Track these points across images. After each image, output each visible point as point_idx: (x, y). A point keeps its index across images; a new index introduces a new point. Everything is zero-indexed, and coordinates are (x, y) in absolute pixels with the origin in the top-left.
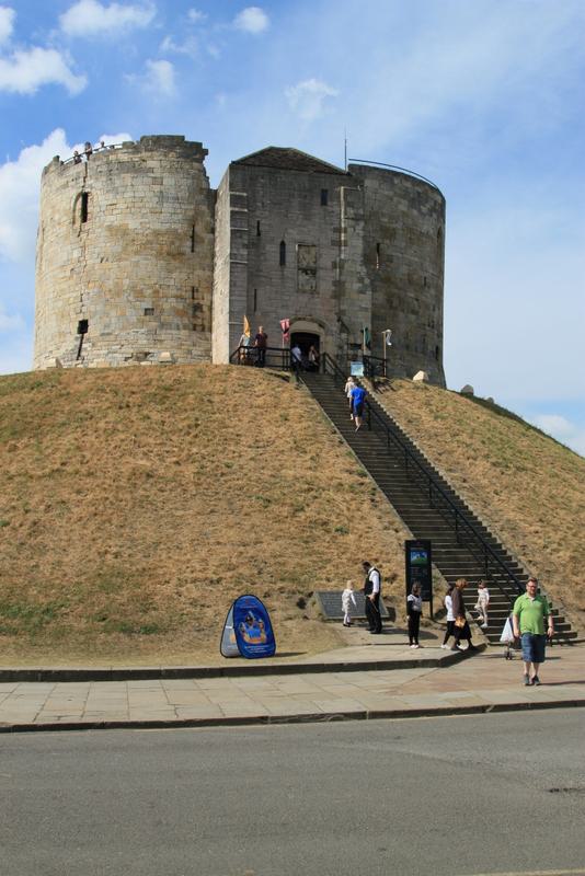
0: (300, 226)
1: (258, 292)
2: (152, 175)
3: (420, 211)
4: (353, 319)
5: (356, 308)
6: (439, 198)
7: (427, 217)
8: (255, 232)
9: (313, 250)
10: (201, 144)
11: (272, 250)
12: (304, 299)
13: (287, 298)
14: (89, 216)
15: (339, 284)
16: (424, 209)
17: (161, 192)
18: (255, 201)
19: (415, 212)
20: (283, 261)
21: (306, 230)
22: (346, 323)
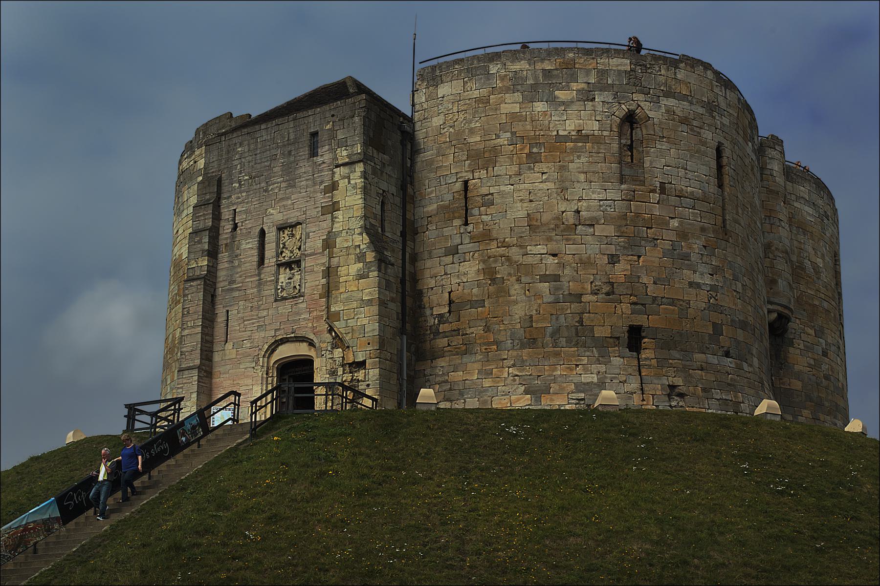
0: (282, 199)
3: (552, 100)
4: (351, 323)
7: (578, 106)
12: (285, 308)
13: (265, 313)
15: (329, 272)
16: (561, 95)
19: (540, 107)
21: (290, 202)
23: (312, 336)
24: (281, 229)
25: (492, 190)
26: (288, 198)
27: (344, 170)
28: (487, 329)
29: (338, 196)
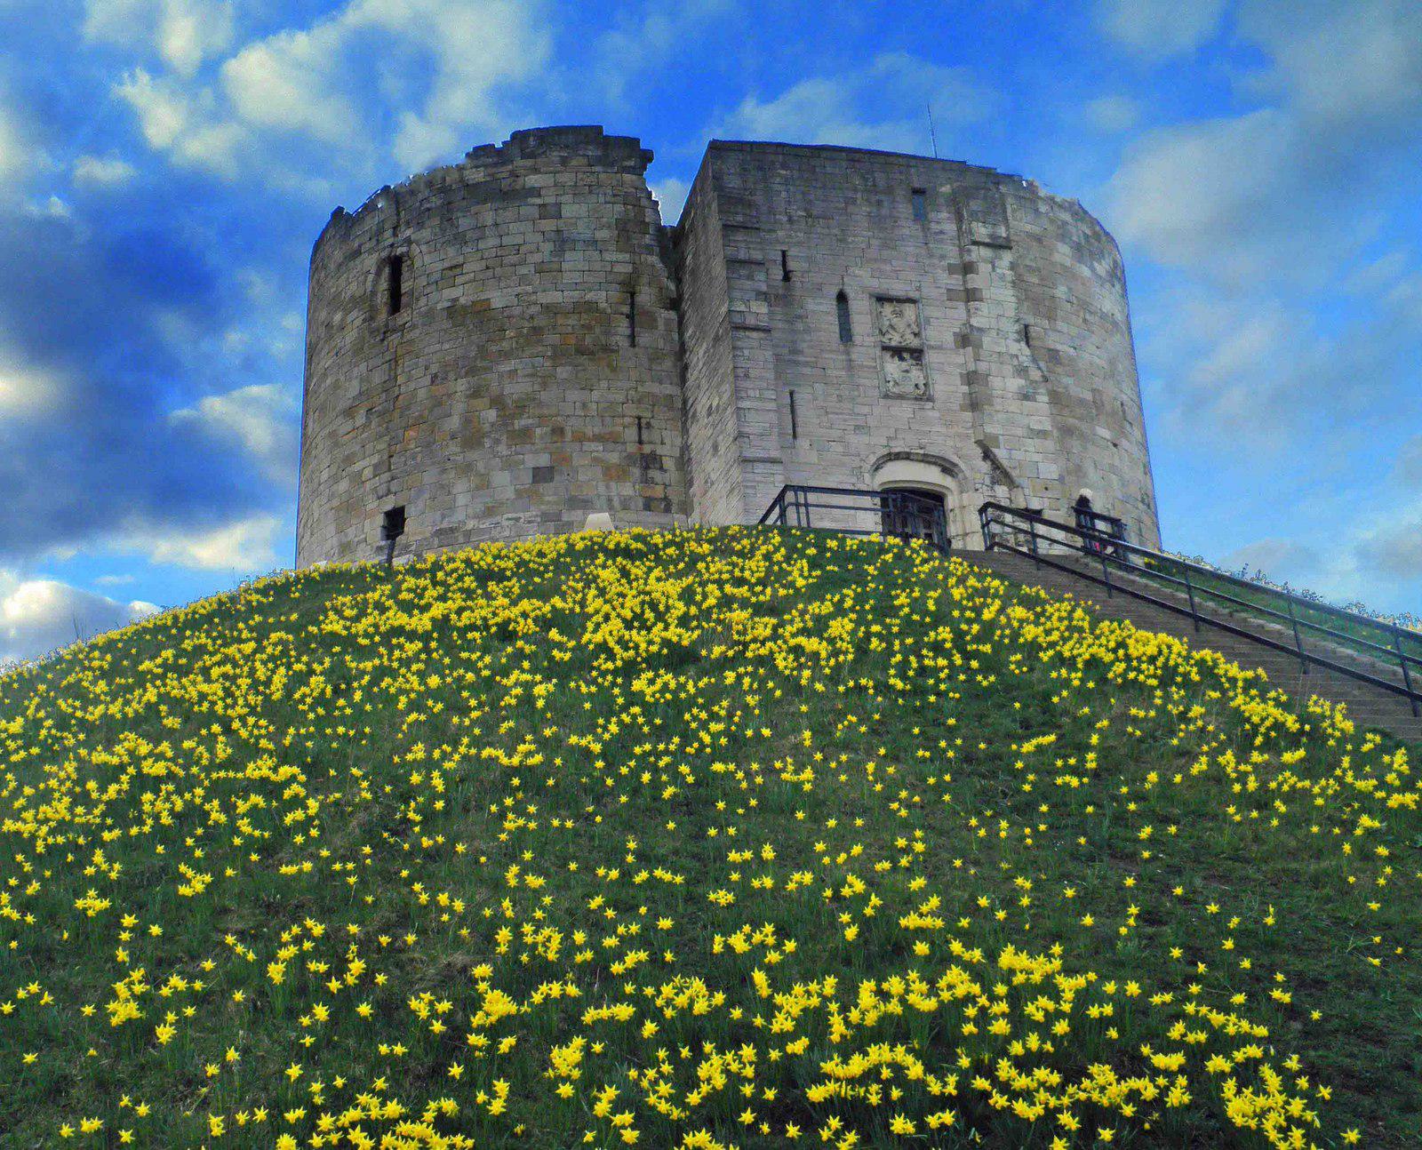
1: (796, 396)
2: (538, 201)
3: (1093, 270)
4: (1017, 455)
5: (1019, 432)
7: (1108, 285)
8: (779, 274)
9: (909, 311)
10: (637, 140)
12: (904, 410)
13: (866, 410)
14: (404, 300)
15: (971, 378)
17: (558, 231)
18: (772, 211)
19: (1086, 272)
20: (846, 334)
21: (888, 268)
22: (1005, 463)
23: (955, 459)
24: (882, 299)
25: (1059, 347)
26: (884, 261)
27: (986, 252)
29: (975, 281)
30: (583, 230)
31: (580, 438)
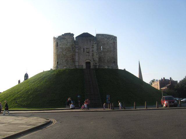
6: (114, 37)
11: (82, 50)
15: (92, 54)
16: (110, 39)
19: (108, 40)
20: (84, 51)
24: (86, 48)
28: (104, 60)
29: (94, 46)
30: (69, 42)
31: (69, 57)
